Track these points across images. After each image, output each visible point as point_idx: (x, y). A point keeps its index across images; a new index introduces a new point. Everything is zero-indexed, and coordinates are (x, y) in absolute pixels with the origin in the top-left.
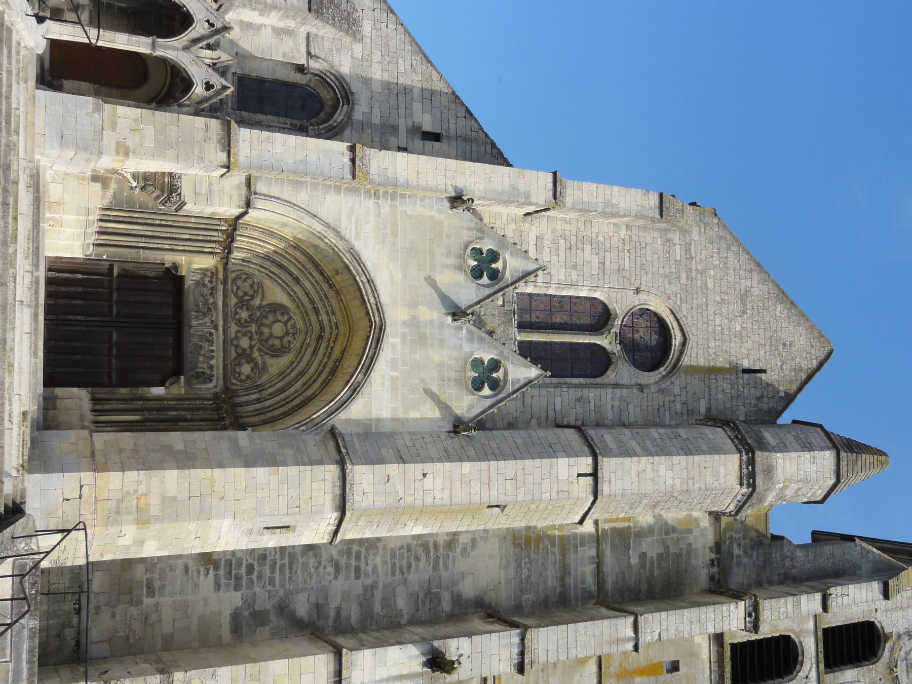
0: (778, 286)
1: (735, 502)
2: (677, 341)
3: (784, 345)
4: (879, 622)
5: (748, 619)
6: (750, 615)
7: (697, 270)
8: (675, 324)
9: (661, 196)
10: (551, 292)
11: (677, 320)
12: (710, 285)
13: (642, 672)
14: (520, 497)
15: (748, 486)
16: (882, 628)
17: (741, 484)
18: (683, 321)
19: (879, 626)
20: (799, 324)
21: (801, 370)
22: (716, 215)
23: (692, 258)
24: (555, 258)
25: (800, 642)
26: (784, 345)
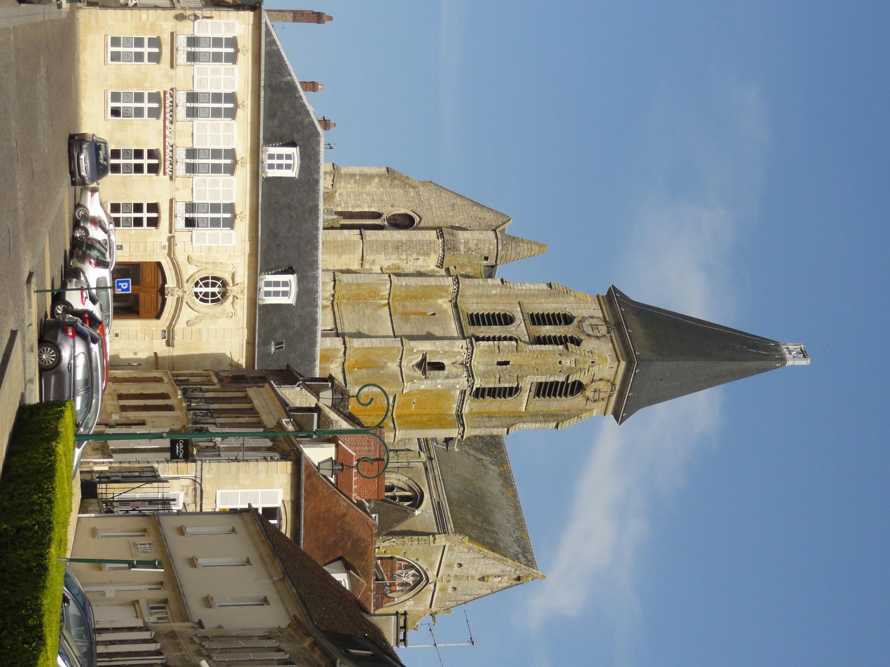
0: (472, 201)
1: (441, 249)
2: (417, 219)
3: (480, 219)
4: (569, 312)
5: (454, 282)
6: (455, 281)
7: (424, 199)
8: (416, 215)
9: (387, 168)
10: (350, 210)
11: (416, 214)
12: (432, 202)
13: (414, 314)
14: (328, 239)
15: (441, 238)
16: (571, 314)
17: (438, 238)
18: (419, 213)
19: (570, 314)
20: (489, 212)
21: (492, 226)
22: (431, 182)
23: (420, 195)
24: (349, 199)
25: (513, 315)
26: (480, 219)
